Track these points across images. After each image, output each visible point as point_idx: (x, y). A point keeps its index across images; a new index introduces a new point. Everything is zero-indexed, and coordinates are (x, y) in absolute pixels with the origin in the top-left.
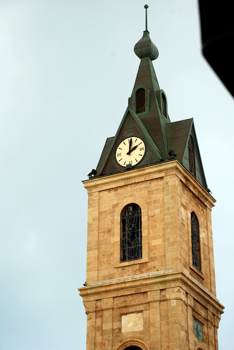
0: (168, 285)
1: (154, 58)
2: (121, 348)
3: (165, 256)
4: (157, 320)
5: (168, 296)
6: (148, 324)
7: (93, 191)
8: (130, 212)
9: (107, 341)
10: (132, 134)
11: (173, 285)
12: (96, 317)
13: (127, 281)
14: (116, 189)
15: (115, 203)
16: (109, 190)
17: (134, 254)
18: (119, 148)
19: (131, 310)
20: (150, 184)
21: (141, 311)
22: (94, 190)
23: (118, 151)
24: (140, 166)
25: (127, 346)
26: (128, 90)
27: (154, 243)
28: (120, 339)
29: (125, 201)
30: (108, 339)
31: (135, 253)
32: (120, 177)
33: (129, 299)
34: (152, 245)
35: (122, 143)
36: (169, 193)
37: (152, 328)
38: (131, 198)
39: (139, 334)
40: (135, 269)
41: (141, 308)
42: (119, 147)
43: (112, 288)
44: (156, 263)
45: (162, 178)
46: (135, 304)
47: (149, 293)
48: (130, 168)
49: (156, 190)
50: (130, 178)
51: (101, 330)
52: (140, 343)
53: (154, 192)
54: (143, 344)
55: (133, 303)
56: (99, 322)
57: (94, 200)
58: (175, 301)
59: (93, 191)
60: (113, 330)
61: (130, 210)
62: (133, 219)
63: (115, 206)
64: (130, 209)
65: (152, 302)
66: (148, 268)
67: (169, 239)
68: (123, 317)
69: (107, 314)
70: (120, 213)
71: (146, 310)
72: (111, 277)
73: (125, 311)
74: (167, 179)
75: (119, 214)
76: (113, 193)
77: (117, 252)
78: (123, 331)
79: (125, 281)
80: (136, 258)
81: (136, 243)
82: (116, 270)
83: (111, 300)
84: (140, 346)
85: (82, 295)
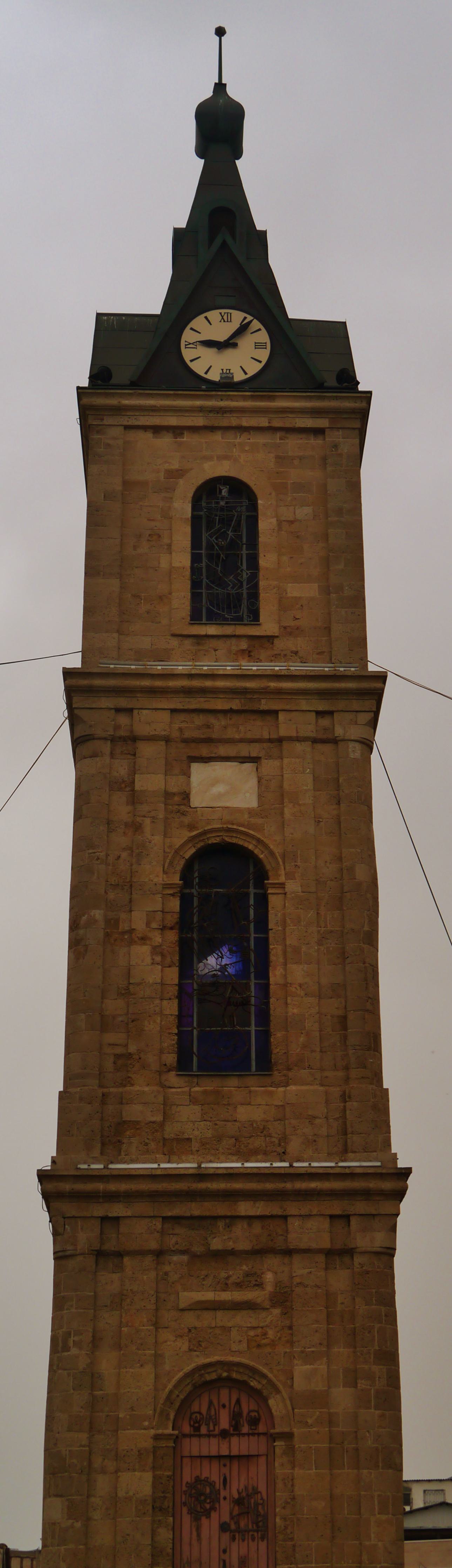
0: (341, 704)
2: (190, 845)
3: (328, 629)
4: (305, 788)
5: (339, 731)
6: (273, 795)
7: (105, 422)
9: (148, 821)
11: (355, 705)
12: (112, 755)
13: (221, 672)
14: (177, 431)
15: (175, 465)
16: (157, 430)
18: (192, 329)
19: (222, 750)
20: (281, 439)
21: (255, 760)
22: (108, 421)
23: (188, 336)
24: (254, 385)
25: (210, 842)
27: (294, 590)
28: (186, 820)
29: (207, 465)
30: (153, 814)
32: (198, 403)
33: (218, 723)
37: (291, 805)
39: (246, 816)
40: (234, 648)
41: (254, 750)
42: (194, 324)
43: (172, 683)
44: (301, 644)
46: (237, 737)
47: (281, 716)
48: (227, 385)
49: (301, 458)
50: (225, 412)
51: (128, 789)
52: (253, 837)
53: (296, 462)
54: (259, 841)
55: (231, 733)
56: (121, 768)
57: (108, 445)
58: (358, 746)
59: (105, 422)
60: (168, 795)
63: (176, 475)
64: (221, 491)
65: (290, 739)
66: (276, 652)
69: (147, 750)
70: (190, 495)
71: (269, 757)
72: (162, 656)
73: (204, 751)
74: (333, 437)
76: (166, 441)
78: (196, 801)
79: (216, 672)
81: (239, 581)
82: (175, 642)
83: (166, 716)
84: (251, 847)
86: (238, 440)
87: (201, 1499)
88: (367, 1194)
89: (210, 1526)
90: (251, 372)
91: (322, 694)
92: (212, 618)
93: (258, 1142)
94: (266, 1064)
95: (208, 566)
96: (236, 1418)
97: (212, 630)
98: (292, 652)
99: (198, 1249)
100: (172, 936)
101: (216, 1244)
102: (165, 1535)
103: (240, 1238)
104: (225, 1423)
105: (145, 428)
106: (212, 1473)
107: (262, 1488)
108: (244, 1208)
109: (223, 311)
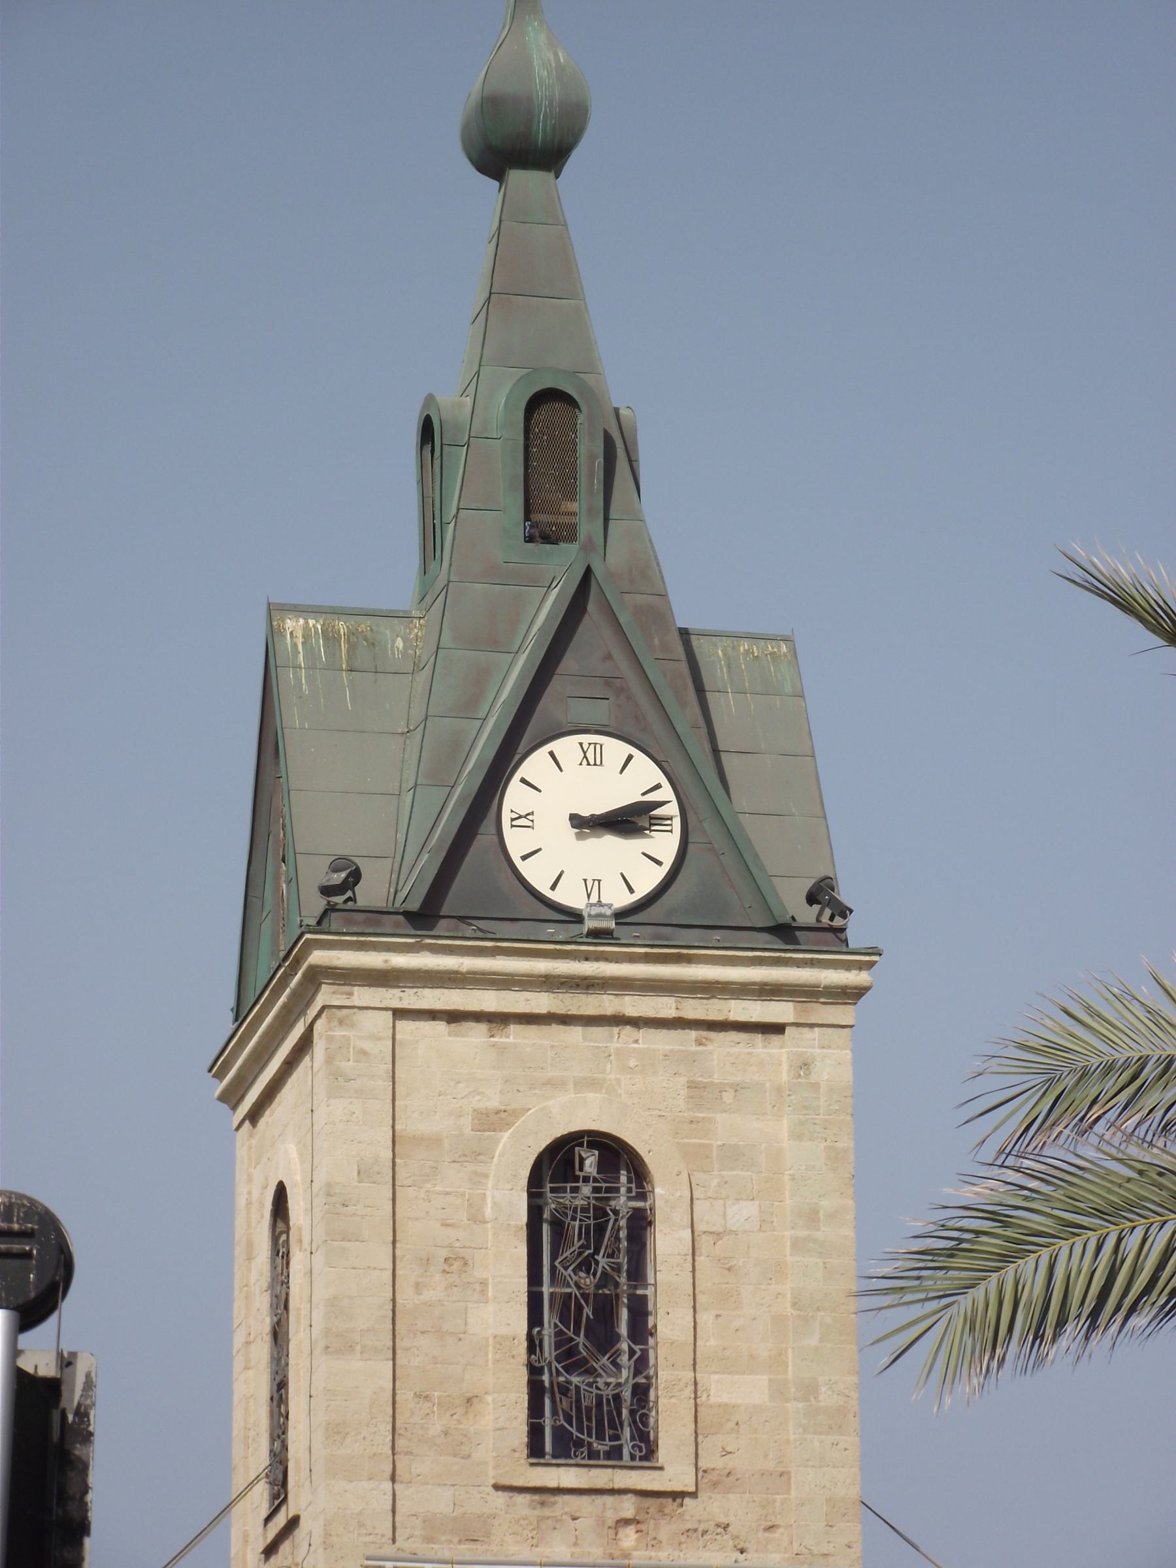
8: (586, 1179)
10: (600, 712)
15: (494, 1103)
16: (454, 1017)
17: (608, 1432)
20: (699, 1043)
22: (363, 995)
26: (447, 361)
27: (722, 1389)
31: (612, 1426)
32: (542, 966)
34: (713, 1400)
35: (542, 753)
36: (817, 1128)
38: (594, 1097)
40: (611, 1517)
42: (524, 771)
45: (777, 1029)
49: (737, 1088)
53: (728, 1097)
57: (364, 1053)
61: (581, 1169)
62: (600, 1229)
63: (493, 1121)
64: (582, 1161)
66: (689, 1526)
67: (809, 1390)
75: (524, 1182)
77: (513, 1396)
80: (615, 1454)
86: (615, 1045)
90: (644, 887)
92: (567, 1448)
95: (559, 1333)
97: (568, 1476)
98: (718, 1526)
105: (432, 1015)
109: (586, 738)
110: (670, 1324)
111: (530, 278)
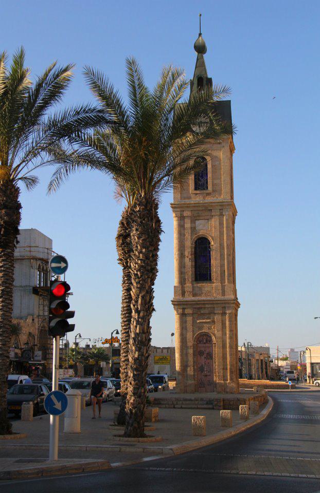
1: (205, 53)
68: (197, 222)
69: (186, 220)
73: (198, 218)
85: (172, 207)
87: (201, 353)
88: (228, 303)
89: (203, 357)
91: (221, 205)
93: (209, 294)
94: (210, 280)
96: (207, 340)
97: (198, 192)
99: (199, 313)
100: (193, 256)
101: (202, 312)
102: (195, 359)
103: (206, 311)
104: (205, 342)
106: (203, 349)
107: (211, 351)
108: (207, 306)
110: (210, 175)
111: (200, 64)
